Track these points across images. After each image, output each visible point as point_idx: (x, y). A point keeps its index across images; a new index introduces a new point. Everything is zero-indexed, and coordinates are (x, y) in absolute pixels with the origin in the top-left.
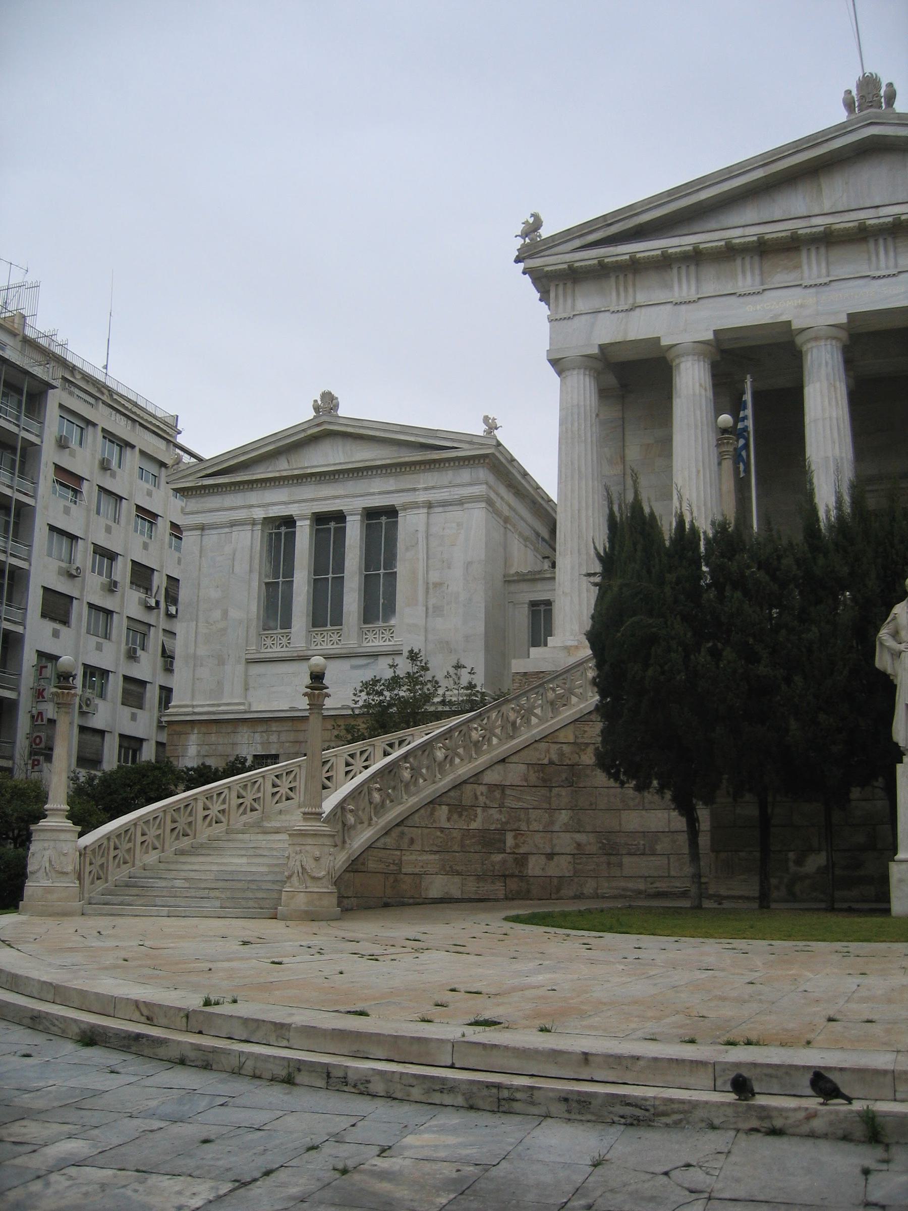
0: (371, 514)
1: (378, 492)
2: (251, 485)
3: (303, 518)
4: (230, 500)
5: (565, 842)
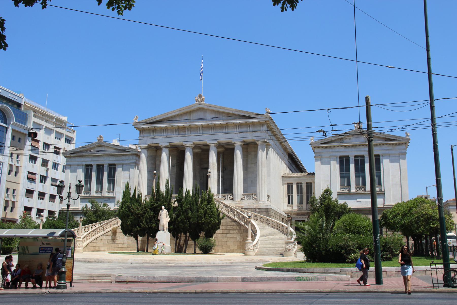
0: (110, 165)
1: (112, 160)
2: (82, 156)
3: (94, 165)
4: (77, 159)
5: (126, 242)
